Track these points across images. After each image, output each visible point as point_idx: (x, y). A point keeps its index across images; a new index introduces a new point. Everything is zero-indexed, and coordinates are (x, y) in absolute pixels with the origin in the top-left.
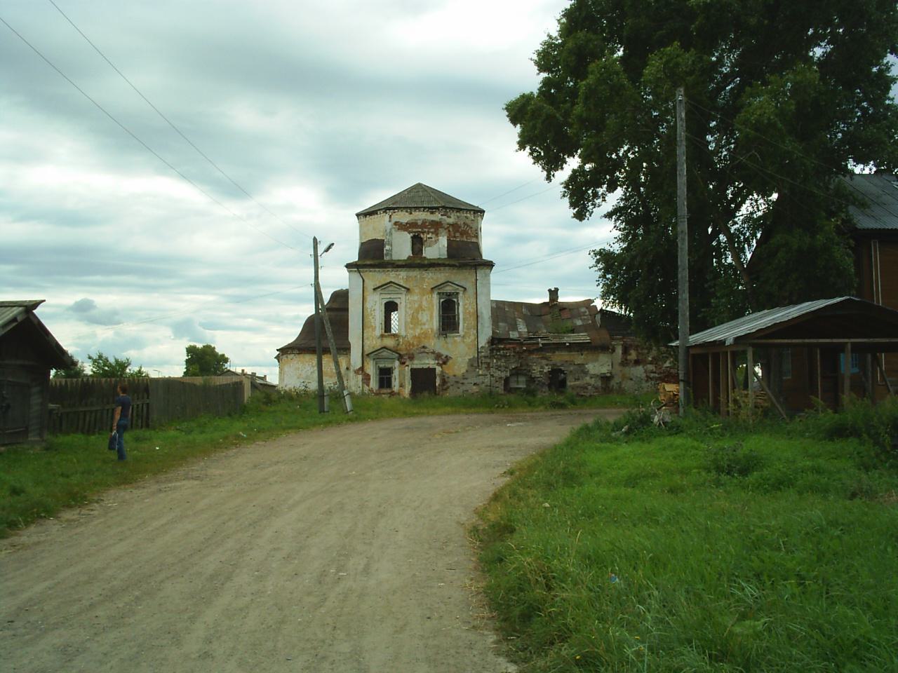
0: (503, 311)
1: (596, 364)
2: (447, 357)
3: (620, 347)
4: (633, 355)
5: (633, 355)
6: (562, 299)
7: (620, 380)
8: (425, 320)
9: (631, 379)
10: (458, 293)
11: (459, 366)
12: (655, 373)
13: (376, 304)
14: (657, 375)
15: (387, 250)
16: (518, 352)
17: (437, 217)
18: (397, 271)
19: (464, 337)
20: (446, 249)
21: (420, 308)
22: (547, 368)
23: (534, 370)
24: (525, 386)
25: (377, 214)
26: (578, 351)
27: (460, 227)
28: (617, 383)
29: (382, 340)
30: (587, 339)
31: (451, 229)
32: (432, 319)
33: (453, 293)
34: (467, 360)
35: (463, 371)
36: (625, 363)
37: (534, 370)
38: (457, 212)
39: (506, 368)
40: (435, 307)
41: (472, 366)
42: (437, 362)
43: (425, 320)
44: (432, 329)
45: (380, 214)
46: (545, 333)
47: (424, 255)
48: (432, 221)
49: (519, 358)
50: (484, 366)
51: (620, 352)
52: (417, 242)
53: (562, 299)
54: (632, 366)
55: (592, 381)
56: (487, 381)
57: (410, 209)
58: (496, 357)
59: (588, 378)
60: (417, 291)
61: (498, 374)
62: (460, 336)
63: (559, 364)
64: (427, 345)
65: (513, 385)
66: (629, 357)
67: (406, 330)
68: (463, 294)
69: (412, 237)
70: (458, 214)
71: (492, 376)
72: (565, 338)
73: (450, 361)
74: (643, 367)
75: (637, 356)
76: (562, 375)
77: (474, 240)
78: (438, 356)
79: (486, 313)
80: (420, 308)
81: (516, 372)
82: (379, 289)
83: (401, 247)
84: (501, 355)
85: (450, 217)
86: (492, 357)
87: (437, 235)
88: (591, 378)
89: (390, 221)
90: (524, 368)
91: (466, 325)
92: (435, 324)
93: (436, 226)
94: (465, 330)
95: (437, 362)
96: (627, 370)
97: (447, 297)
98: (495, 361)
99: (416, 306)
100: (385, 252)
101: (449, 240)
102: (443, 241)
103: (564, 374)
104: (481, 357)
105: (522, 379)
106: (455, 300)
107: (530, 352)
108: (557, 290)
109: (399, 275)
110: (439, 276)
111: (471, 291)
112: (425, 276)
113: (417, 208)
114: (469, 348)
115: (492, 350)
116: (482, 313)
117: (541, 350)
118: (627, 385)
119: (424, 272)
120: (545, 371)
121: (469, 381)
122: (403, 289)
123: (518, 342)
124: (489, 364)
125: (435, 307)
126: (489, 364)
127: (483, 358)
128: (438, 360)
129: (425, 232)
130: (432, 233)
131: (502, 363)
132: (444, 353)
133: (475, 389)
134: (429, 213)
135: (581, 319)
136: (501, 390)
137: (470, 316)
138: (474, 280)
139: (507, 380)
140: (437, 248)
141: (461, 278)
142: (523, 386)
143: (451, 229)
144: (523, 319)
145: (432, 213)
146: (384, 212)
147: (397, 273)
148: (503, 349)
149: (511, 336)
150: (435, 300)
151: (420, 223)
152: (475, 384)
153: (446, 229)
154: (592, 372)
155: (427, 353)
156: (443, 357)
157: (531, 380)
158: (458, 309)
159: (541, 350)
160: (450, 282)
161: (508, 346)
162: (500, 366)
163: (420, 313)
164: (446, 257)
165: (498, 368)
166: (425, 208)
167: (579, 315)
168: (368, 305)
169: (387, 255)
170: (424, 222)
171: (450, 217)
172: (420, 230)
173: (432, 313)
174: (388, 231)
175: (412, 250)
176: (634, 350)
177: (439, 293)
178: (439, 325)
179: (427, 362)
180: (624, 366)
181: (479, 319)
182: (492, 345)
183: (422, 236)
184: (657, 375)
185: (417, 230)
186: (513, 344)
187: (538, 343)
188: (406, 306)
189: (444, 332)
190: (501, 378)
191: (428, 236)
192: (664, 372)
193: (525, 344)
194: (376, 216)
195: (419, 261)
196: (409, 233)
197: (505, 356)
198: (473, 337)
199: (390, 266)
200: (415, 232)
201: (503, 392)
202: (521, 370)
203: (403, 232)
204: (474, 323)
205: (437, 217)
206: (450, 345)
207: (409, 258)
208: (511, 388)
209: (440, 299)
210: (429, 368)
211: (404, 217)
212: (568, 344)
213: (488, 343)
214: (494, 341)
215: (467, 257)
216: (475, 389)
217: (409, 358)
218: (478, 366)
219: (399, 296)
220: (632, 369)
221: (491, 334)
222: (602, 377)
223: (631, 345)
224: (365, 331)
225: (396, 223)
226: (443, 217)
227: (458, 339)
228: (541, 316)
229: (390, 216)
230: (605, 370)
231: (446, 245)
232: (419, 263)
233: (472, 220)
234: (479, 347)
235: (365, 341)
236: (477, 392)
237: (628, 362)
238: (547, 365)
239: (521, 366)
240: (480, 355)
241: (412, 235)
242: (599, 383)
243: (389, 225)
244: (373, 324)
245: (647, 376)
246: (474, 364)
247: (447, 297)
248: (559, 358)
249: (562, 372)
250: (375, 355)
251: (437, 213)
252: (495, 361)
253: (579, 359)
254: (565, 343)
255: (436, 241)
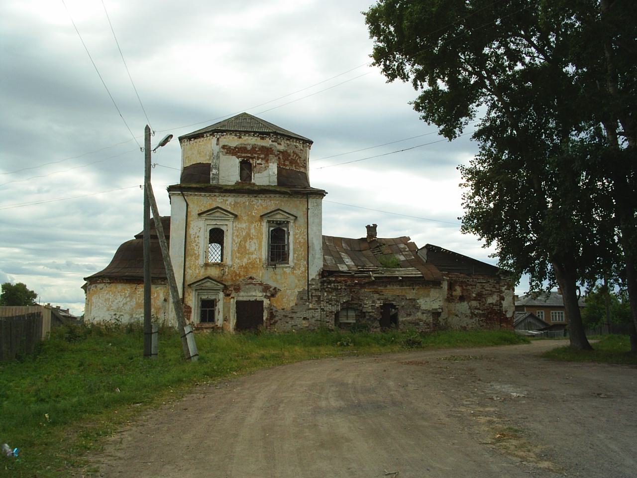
0: (333, 245)
1: (427, 299)
2: (275, 289)
3: (447, 282)
4: (458, 291)
5: (458, 291)
6: (380, 235)
7: (446, 316)
8: (252, 249)
9: (457, 316)
10: (288, 222)
11: (288, 298)
12: (479, 309)
13: (201, 229)
14: (481, 312)
15: (213, 174)
16: (349, 286)
17: (267, 143)
18: (225, 196)
19: (293, 268)
20: (276, 176)
21: (248, 237)
22: (379, 302)
23: (366, 304)
24: (355, 321)
25: (203, 137)
26: (409, 286)
27: (290, 156)
28: (444, 319)
29: (206, 269)
30: (418, 274)
31: (281, 157)
32: (260, 249)
33: (284, 222)
34: (297, 293)
35: (292, 304)
36: (450, 299)
37: (366, 304)
38: (287, 140)
39: (337, 301)
40: (264, 236)
41: (302, 298)
42: (264, 294)
43: (252, 249)
44: (260, 260)
45: (207, 136)
46: (374, 270)
47: (253, 181)
48: (263, 147)
49: (351, 292)
50: (315, 299)
51: (446, 288)
52: (246, 168)
53: (380, 235)
54: (458, 303)
55: (424, 317)
56: (317, 314)
57: (239, 133)
58: (327, 290)
59: (419, 314)
60: (245, 218)
61: (329, 308)
62: (289, 267)
63: (390, 299)
64: (254, 276)
65: (343, 320)
66: (454, 293)
67: (232, 259)
68: (294, 222)
69: (241, 163)
70: (288, 142)
71: (323, 310)
72: (397, 273)
73: (279, 294)
74: (468, 303)
75: (462, 292)
76: (393, 310)
77: (302, 170)
78: (266, 288)
79: (317, 245)
80: (248, 237)
81: (347, 307)
82: (205, 215)
83: (229, 171)
84: (332, 289)
85: (281, 144)
86: (322, 290)
87: (267, 161)
88: (423, 313)
89: (217, 144)
90: (355, 302)
91: (296, 255)
92: (264, 253)
93: (267, 152)
94: (295, 261)
95: (264, 294)
96: (452, 305)
97: (278, 226)
98: (326, 294)
99: (244, 234)
100: (211, 175)
101: (278, 167)
102: (273, 168)
103: (395, 309)
104: (311, 289)
105: (352, 313)
106: (286, 229)
107: (362, 286)
108: (375, 226)
109: (227, 200)
110: (269, 203)
111: (302, 220)
112: (254, 203)
113: (247, 132)
114: (299, 280)
115: (323, 283)
116: (313, 244)
117: (372, 283)
118: (454, 320)
119: (253, 199)
120: (377, 305)
121: (298, 315)
122: (231, 216)
123: (348, 275)
124: (319, 297)
125: (264, 236)
126: (319, 297)
127: (314, 291)
128: (266, 292)
129: (254, 157)
130: (262, 159)
131: (333, 296)
132: (273, 284)
133: (305, 324)
134: (259, 139)
135: (403, 254)
136: (331, 325)
137: (301, 247)
138: (305, 210)
139: (337, 315)
140: (267, 175)
141: (292, 206)
142: (352, 321)
143: (281, 157)
144: (346, 253)
145: (262, 138)
146: (211, 135)
147: (225, 198)
148: (334, 282)
149: (341, 269)
150: (265, 229)
151: (249, 148)
152: (304, 319)
153: (276, 156)
154: (423, 307)
155: (255, 285)
156: (271, 289)
157: (362, 314)
158: (288, 238)
159: (372, 283)
160: (281, 210)
161: (339, 279)
162: (331, 300)
163: (248, 241)
164: (276, 184)
165: (329, 302)
166: (255, 132)
167: (400, 251)
168: (191, 231)
169: (214, 179)
170: (254, 147)
171: (281, 144)
172: (249, 155)
173: (261, 242)
174: (215, 154)
175: (240, 176)
176: (459, 286)
177: (269, 222)
178: (268, 255)
179: (254, 294)
180: (449, 302)
181: (310, 249)
182: (323, 277)
183: (251, 161)
184: (481, 312)
185: (246, 155)
186: (343, 276)
187: (370, 277)
188: (233, 233)
189: (273, 263)
190: (332, 312)
191: (258, 162)
192: (488, 309)
193: (357, 277)
194: (202, 139)
195: (248, 187)
196: (238, 158)
197: (336, 289)
198: (303, 269)
199: (217, 190)
200: (244, 157)
201: (333, 327)
202: (352, 304)
203: (231, 157)
204: (304, 254)
205: (267, 143)
206: (278, 277)
207: (237, 183)
208: (341, 323)
209: (269, 227)
210: (256, 300)
211: (232, 141)
212: (401, 278)
213: (319, 275)
214: (325, 273)
215: (296, 187)
216: (305, 324)
217: (235, 289)
218: (309, 299)
219: (227, 223)
220: (457, 305)
221: (322, 266)
222: (433, 313)
223: (456, 282)
224: (187, 259)
225: (224, 147)
226: (274, 143)
227: (288, 270)
228: (360, 251)
229: (218, 139)
230: (436, 306)
231: (276, 172)
232: (248, 189)
233: (301, 150)
234: (310, 279)
235: (188, 270)
236: (306, 327)
237: (454, 298)
238: (378, 299)
239: (352, 300)
240: (310, 288)
241: (240, 159)
242: (431, 319)
243: (216, 149)
244: (196, 252)
245: (472, 313)
246: (305, 297)
247: (278, 226)
248: (391, 292)
249: (393, 306)
250: (198, 285)
251: (268, 139)
252: (326, 294)
253: (410, 293)
254: (397, 277)
255: (266, 168)
